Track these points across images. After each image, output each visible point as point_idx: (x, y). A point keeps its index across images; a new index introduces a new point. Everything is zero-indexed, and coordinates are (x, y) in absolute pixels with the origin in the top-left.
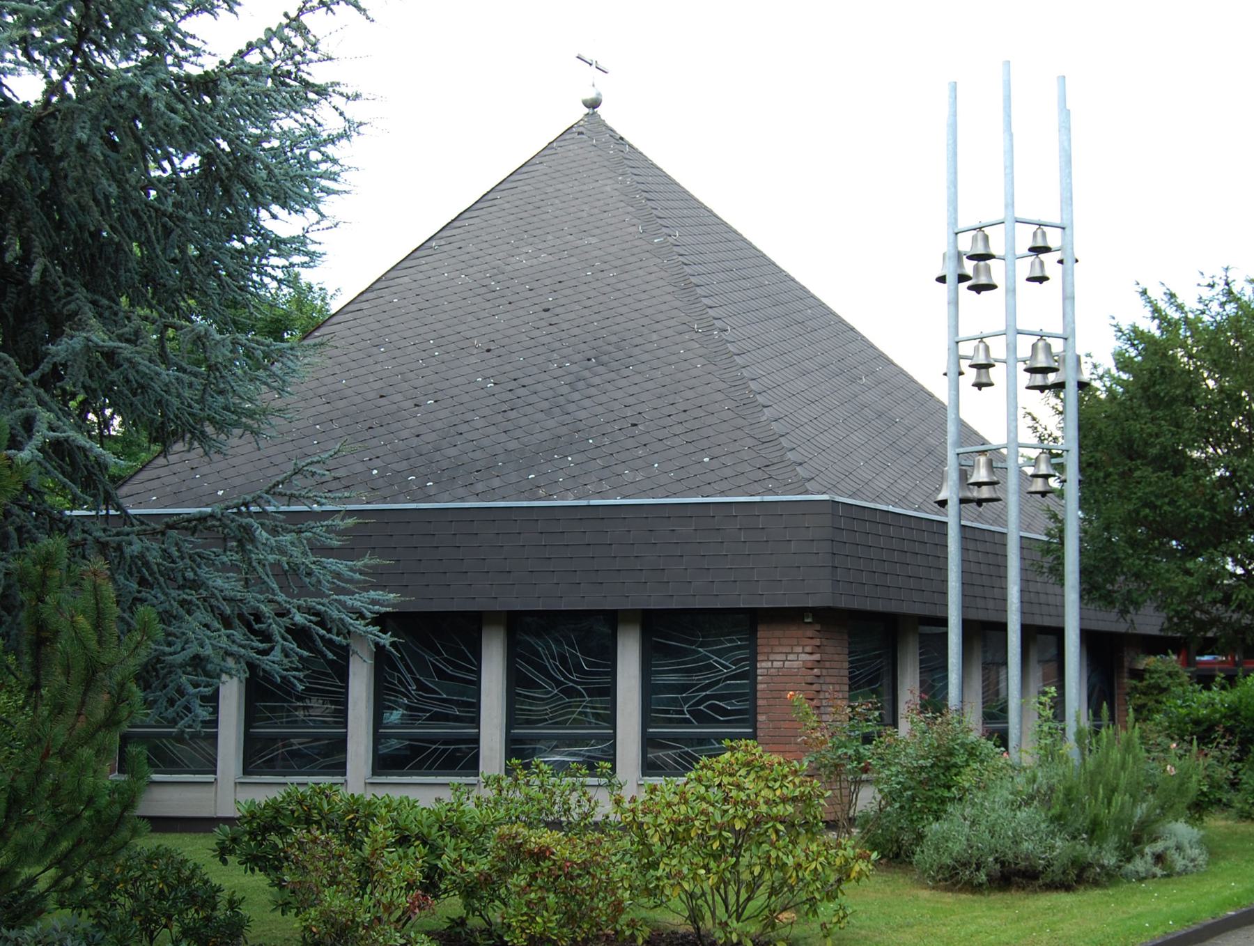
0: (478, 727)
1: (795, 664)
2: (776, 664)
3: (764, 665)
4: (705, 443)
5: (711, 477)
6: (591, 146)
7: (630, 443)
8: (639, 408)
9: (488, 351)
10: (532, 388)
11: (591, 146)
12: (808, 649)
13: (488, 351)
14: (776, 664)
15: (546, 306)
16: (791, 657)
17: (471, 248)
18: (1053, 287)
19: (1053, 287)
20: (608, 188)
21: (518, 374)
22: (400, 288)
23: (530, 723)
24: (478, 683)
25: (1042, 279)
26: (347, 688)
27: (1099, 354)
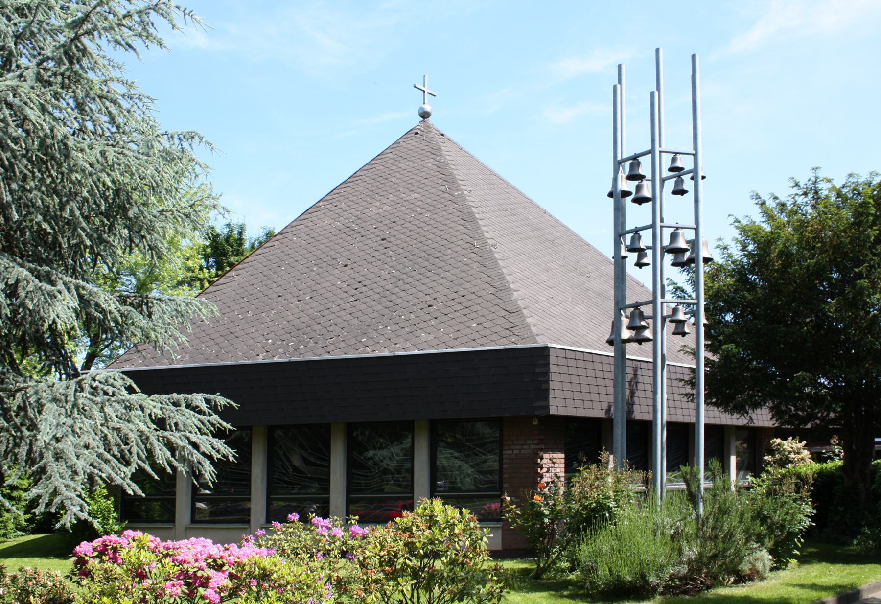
0: (329, 494)
1: (528, 452)
2: (515, 452)
3: (507, 452)
4: (474, 315)
5: (476, 336)
6: (422, 139)
7: (427, 317)
8: (435, 295)
9: (346, 266)
10: (370, 287)
11: (422, 139)
12: (536, 442)
13: (346, 266)
14: (515, 452)
15: (383, 237)
16: (525, 447)
17: (343, 205)
18: (690, 197)
19: (690, 197)
20: (430, 165)
21: (363, 278)
22: (298, 232)
23: (360, 491)
24: (328, 467)
25: (682, 192)
26: (250, 471)
27: (721, 241)
